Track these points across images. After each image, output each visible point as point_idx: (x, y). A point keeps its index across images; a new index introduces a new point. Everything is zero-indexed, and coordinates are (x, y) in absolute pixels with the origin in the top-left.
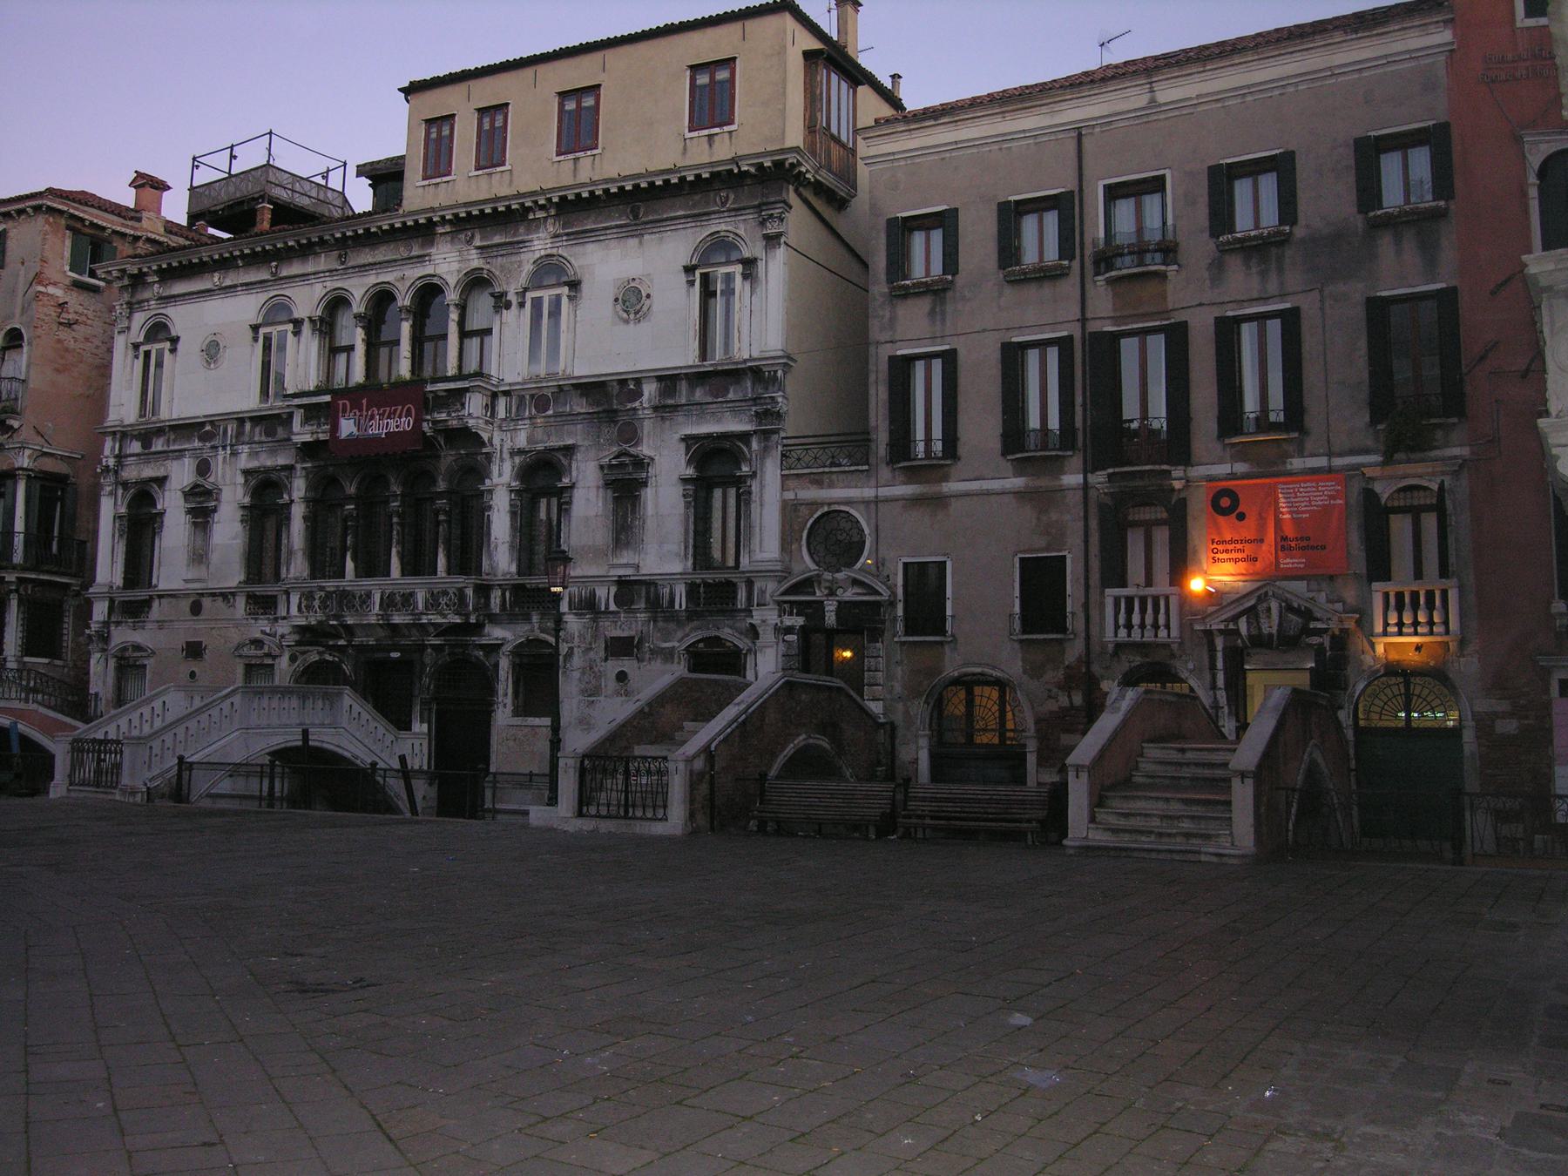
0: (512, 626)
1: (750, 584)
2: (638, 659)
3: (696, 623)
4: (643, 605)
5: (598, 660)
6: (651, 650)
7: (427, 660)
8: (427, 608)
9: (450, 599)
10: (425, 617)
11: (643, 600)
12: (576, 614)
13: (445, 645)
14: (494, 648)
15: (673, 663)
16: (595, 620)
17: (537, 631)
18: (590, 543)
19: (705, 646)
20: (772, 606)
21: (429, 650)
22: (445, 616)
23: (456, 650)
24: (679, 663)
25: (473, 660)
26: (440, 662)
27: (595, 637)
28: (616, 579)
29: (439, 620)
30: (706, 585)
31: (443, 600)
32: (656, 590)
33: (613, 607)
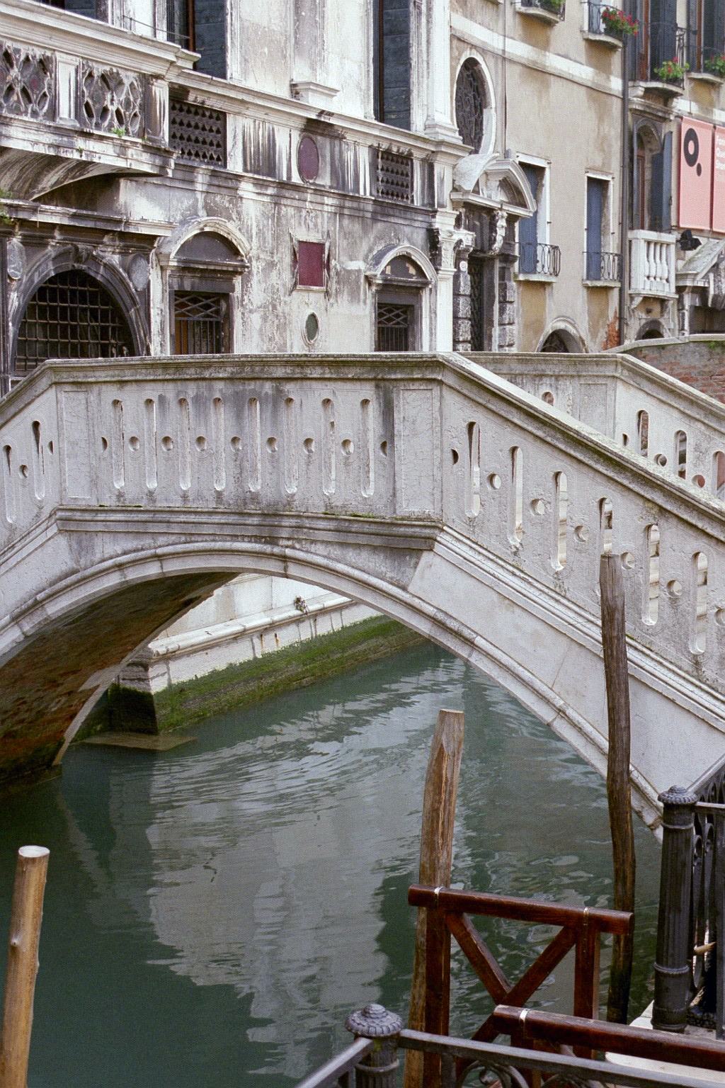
0: (164, 192)
1: (429, 167)
2: (327, 293)
3: (379, 226)
4: (325, 180)
5: (282, 291)
6: (337, 274)
7: (16, 267)
8: (78, 116)
9: (128, 104)
10: (80, 143)
11: (328, 169)
12: (257, 183)
13: (53, 226)
14: (142, 244)
15: (359, 301)
16: (277, 201)
17: (203, 217)
18: (265, 24)
19: (392, 271)
20: (449, 209)
21: (16, 241)
22: (122, 149)
23: (81, 246)
24: (365, 302)
25: (100, 275)
26: (36, 280)
27: (277, 237)
28: (314, 116)
29: (105, 156)
30: (387, 154)
31: (113, 103)
32: (341, 153)
33: (296, 179)
